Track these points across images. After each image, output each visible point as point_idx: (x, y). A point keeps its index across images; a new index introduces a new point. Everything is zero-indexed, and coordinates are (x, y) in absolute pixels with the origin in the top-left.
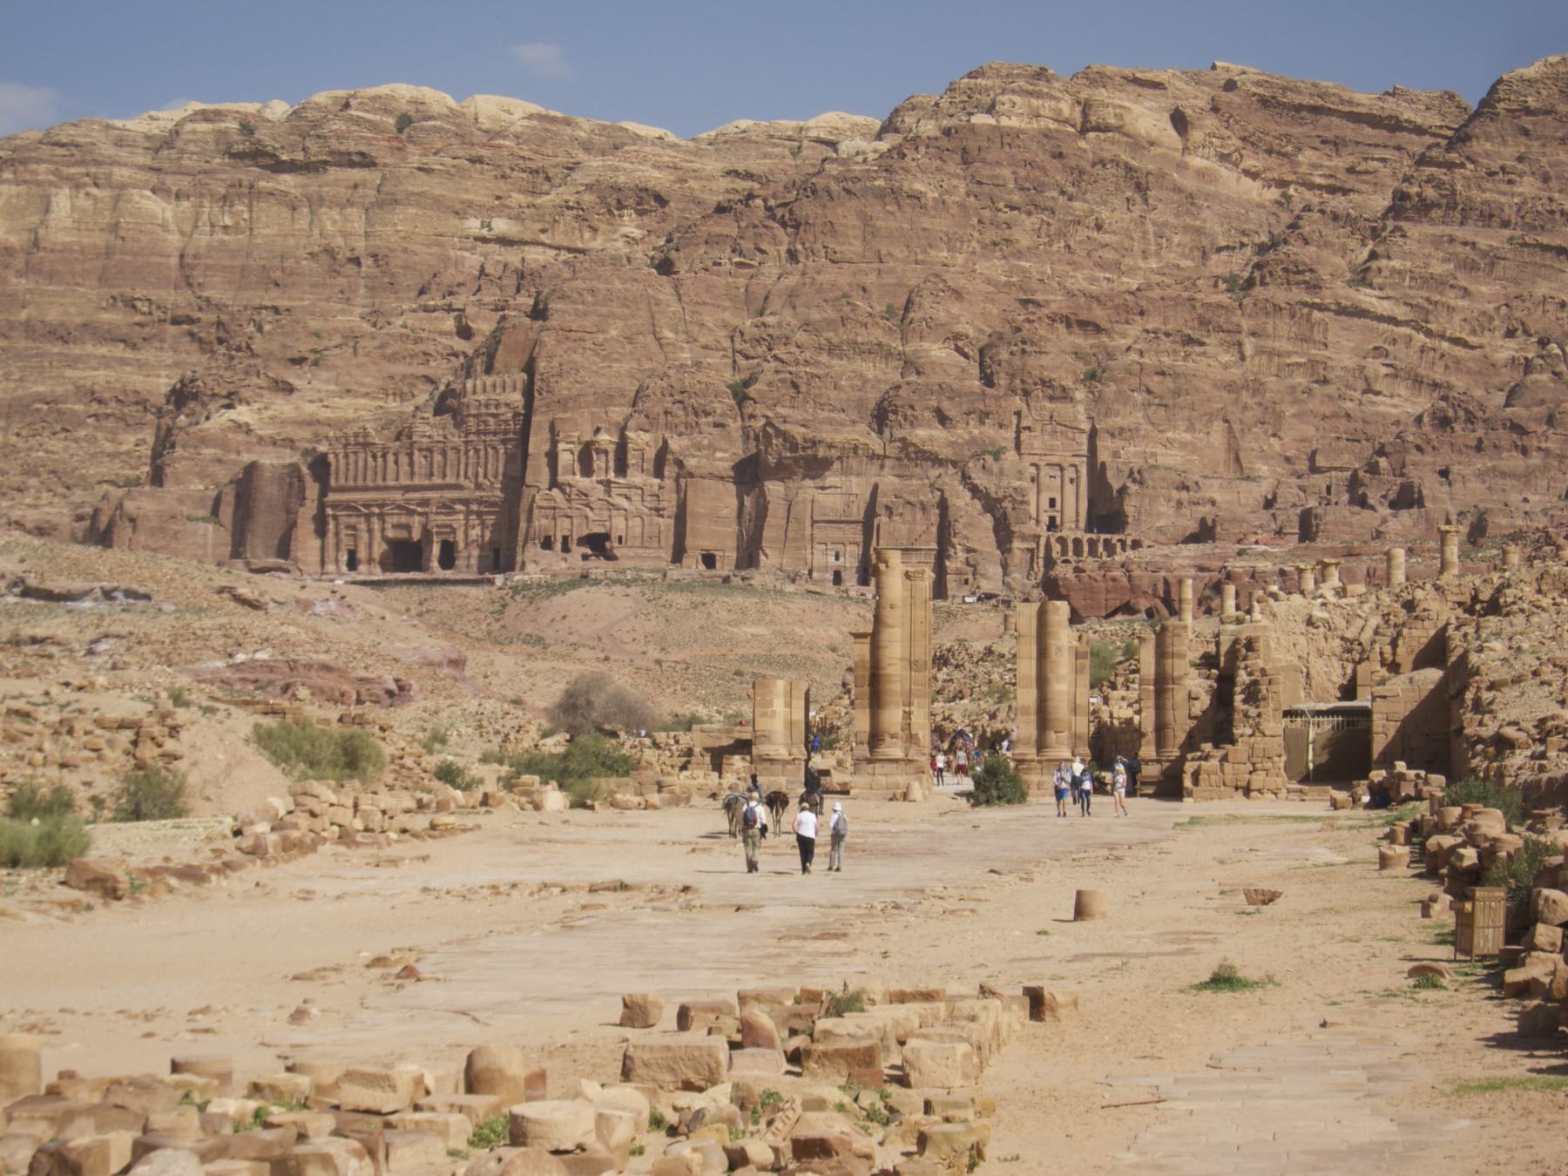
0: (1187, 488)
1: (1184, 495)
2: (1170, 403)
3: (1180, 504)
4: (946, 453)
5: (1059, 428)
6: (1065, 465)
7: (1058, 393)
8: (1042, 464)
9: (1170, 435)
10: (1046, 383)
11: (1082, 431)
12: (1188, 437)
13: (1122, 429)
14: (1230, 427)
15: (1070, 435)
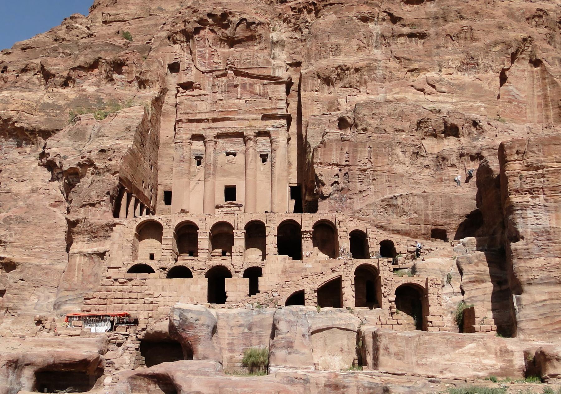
0: (452, 131)
1: (450, 145)
2: (432, 31)
3: (441, 159)
4: (37, 120)
5: (239, 80)
6: (249, 133)
7: (241, 32)
8: (210, 135)
9: (432, 75)
10: (222, 20)
11: (277, 81)
12: (466, 78)
13: (343, 70)
14: (544, 71)
15: (258, 88)
